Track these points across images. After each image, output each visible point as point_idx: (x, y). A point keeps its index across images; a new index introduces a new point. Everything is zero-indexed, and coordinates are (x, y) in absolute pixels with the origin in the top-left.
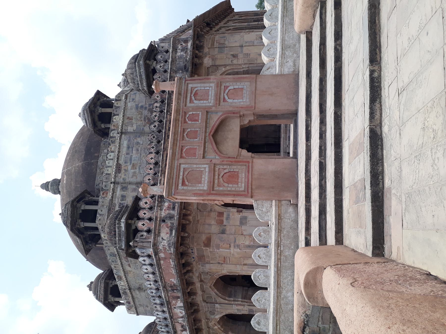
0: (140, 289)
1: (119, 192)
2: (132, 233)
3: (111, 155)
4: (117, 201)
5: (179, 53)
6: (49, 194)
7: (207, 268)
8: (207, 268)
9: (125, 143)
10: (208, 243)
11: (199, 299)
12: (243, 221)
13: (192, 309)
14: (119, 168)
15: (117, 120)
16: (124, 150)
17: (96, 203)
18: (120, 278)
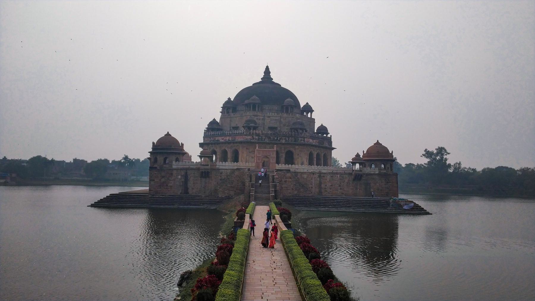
0: (231, 121)
1: (261, 118)
2: (249, 128)
3: (273, 114)
4: (258, 117)
5: (300, 139)
6: (264, 70)
7: (241, 148)
8: (241, 148)
9: (277, 118)
10: (247, 149)
11: (232, 144)
12: (252, 157)
13: (229, 143)
14: (269, 117)
15: (285, 115)
16: (275, 118)
17: (258, 111)
18: (234, 115)
